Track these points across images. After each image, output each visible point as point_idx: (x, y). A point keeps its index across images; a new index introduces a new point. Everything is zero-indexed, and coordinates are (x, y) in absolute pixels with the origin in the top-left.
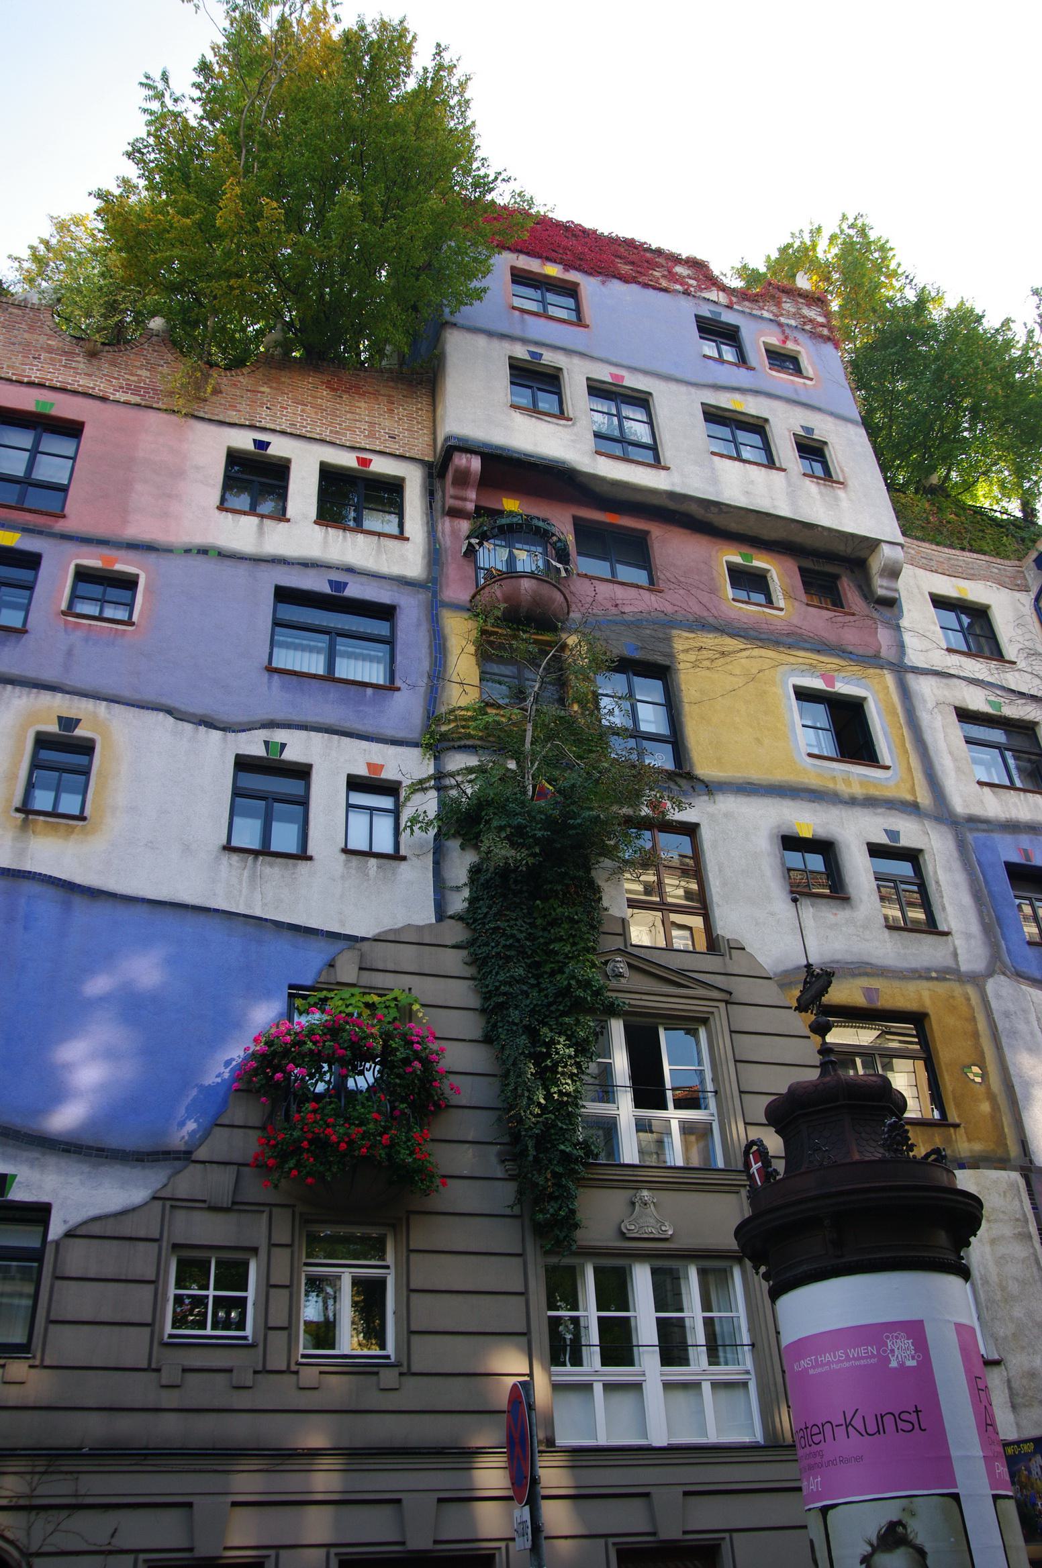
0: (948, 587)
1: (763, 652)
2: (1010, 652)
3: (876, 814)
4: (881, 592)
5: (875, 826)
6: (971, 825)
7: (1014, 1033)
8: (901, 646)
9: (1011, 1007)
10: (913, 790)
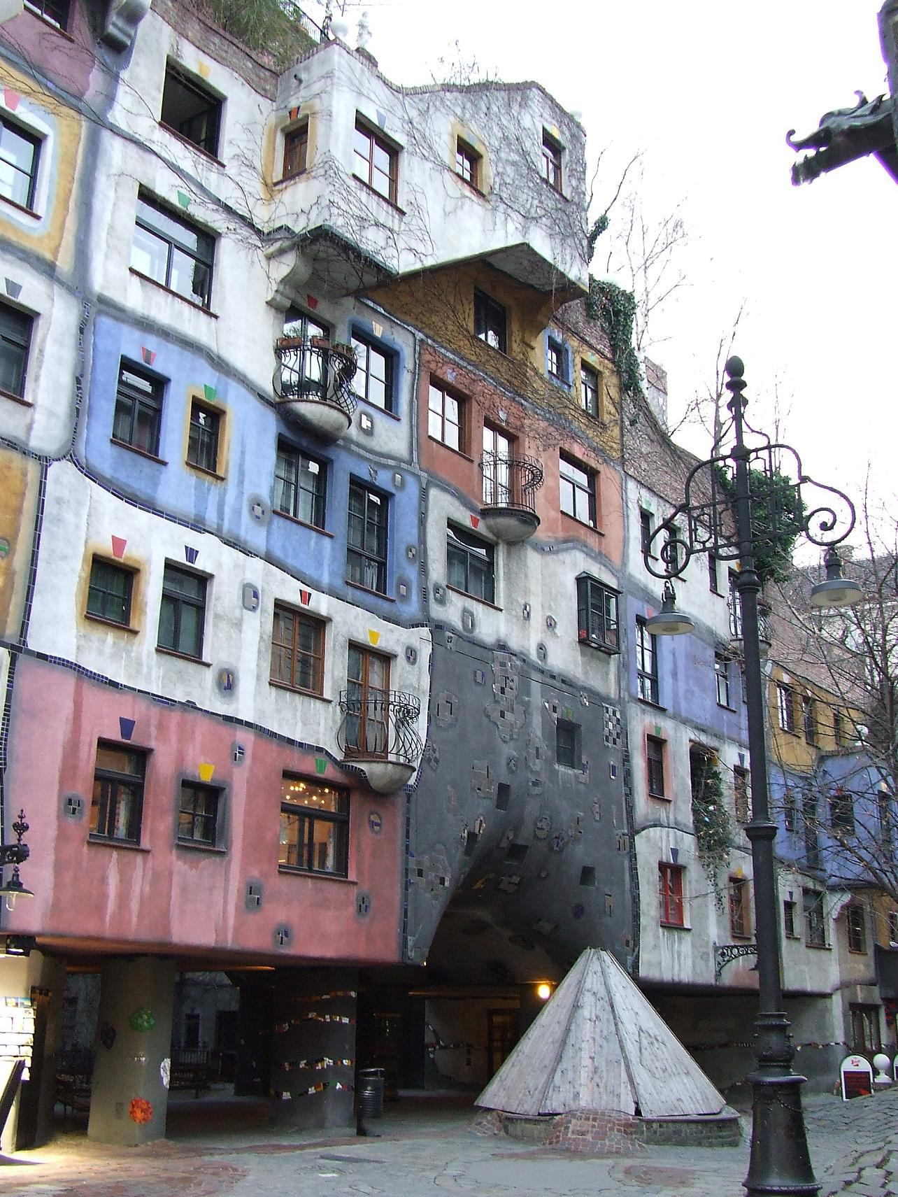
2: (226, 151)
4: (111, 29)
6: (103, 307)
7: (58, 520)
8: (110, 99)
9: (66, 494)
10: (56, 252)
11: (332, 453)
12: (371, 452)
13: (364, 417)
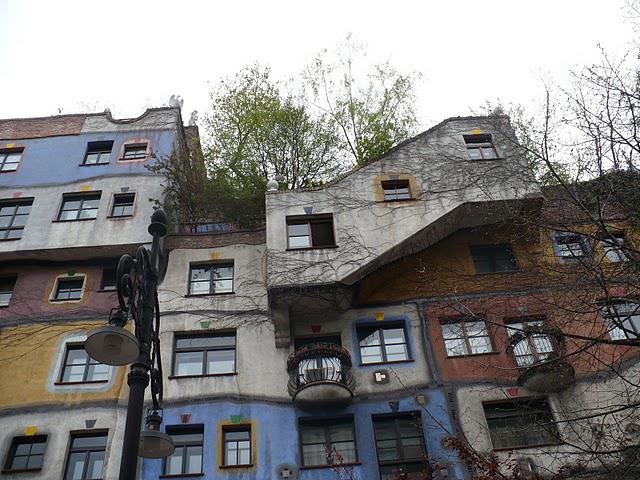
0: (204, 255)
1: (54, 328)
3: (84, 412)
5: (78, 421)
11: (350, 410)
12: (390, 392)
13: (378, 375)
